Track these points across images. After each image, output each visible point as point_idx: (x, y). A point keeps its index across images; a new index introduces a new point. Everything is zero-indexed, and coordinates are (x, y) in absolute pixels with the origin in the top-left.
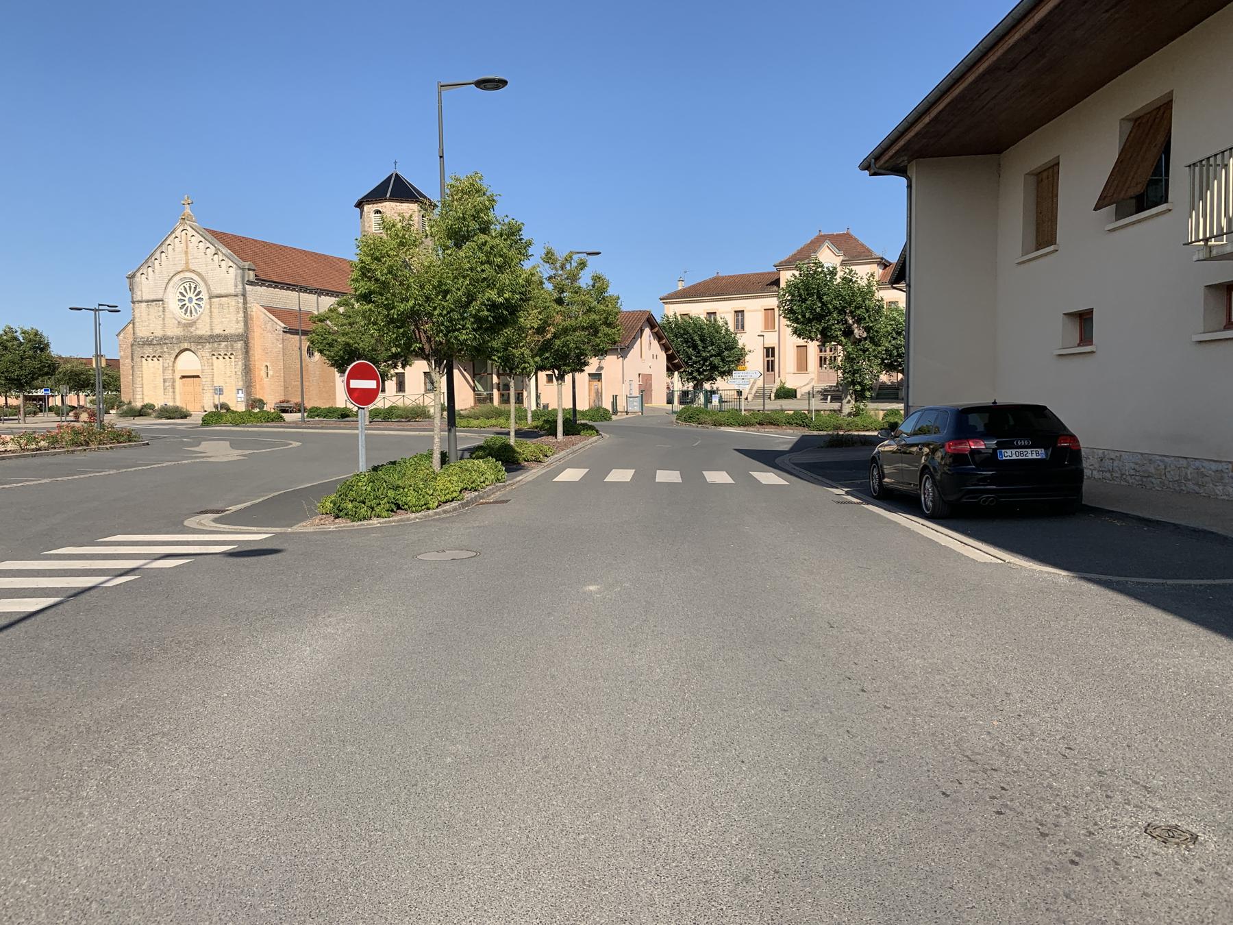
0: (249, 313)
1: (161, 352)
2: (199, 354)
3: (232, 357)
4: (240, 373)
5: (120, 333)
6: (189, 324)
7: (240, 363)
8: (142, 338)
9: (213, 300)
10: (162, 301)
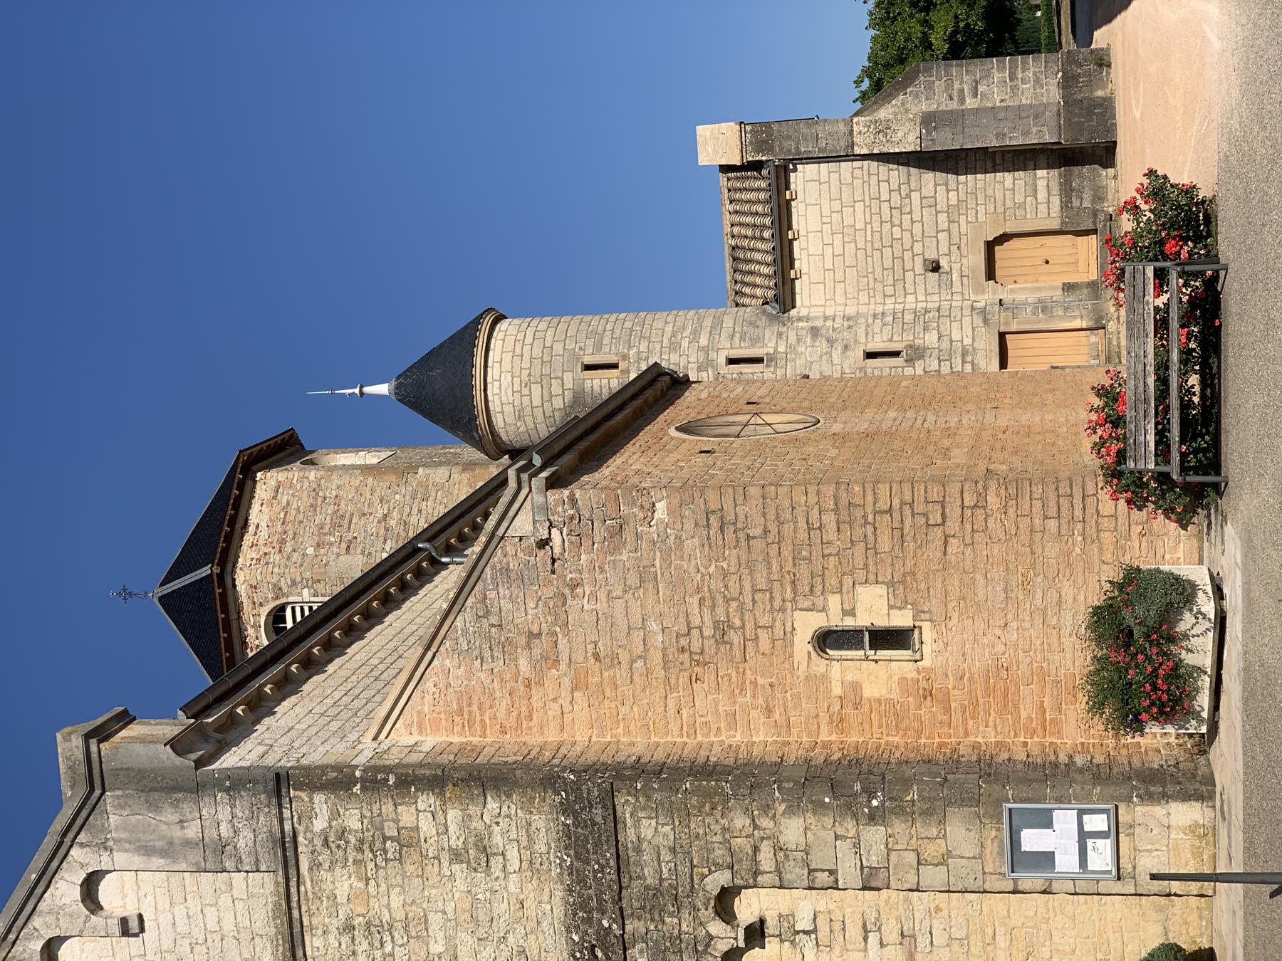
0: (414, 758)
3: (748, 908)
4: (874, 836)
7: (792, 830)
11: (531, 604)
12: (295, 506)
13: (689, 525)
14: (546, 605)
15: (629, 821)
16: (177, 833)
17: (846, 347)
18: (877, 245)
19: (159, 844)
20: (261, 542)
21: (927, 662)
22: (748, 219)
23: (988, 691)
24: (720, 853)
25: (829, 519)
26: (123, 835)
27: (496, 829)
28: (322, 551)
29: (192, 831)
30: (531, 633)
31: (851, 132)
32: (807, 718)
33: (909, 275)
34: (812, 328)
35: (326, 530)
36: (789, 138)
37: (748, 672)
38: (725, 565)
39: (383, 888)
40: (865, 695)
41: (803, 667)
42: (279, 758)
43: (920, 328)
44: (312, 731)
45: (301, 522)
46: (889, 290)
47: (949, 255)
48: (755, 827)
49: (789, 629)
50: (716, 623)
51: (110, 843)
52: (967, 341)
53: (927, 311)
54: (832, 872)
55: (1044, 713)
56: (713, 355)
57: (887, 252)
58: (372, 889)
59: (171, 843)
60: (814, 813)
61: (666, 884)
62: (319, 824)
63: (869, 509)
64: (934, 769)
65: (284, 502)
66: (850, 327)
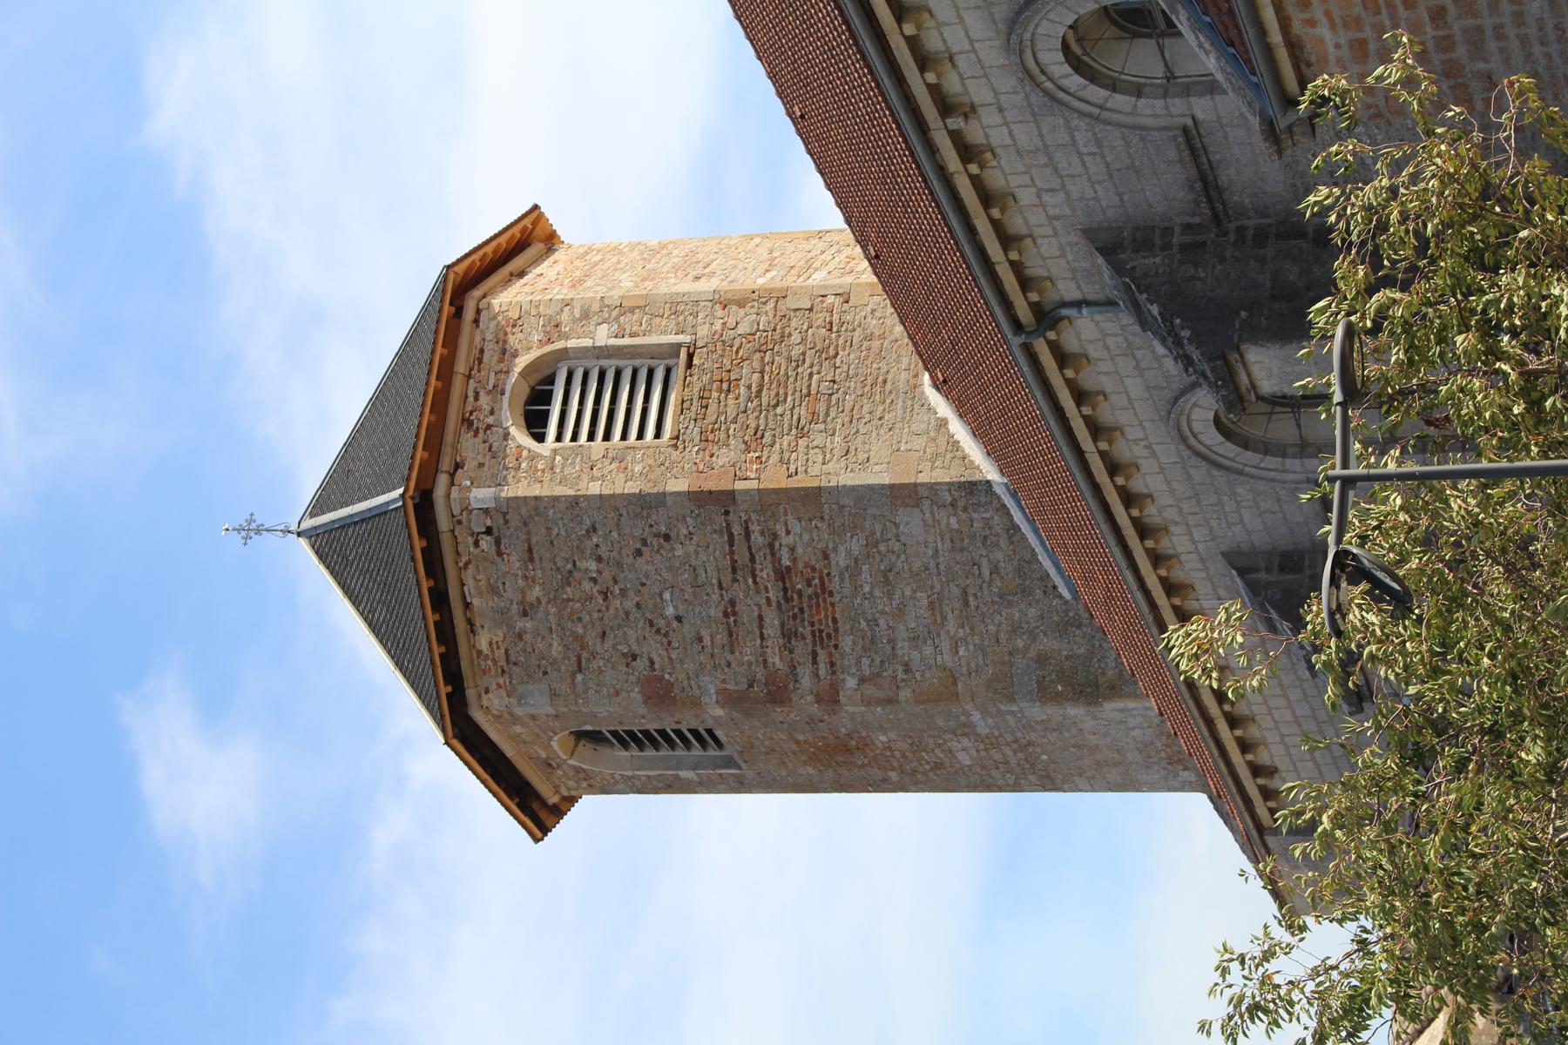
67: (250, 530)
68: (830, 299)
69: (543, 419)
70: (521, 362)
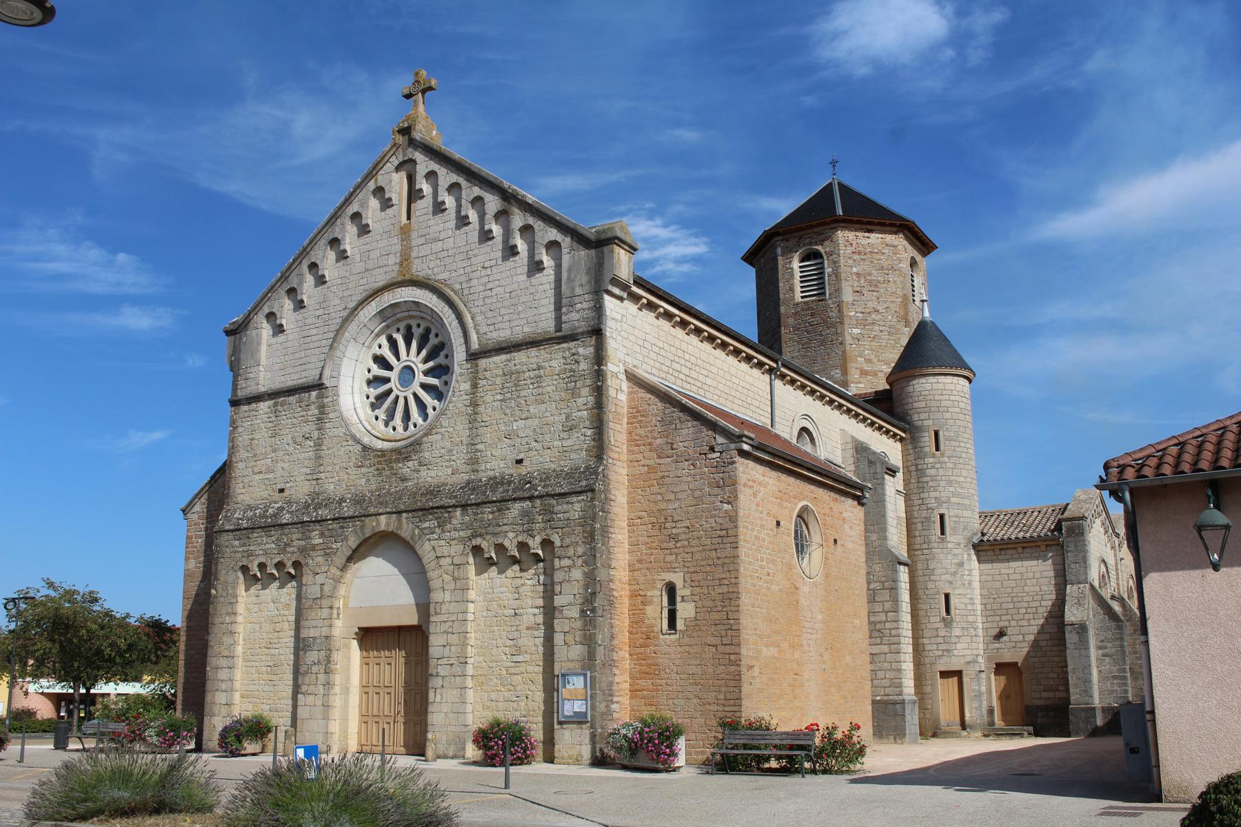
1: (303, 550)
2: (426, 549)
5: (191, 504)
6: (397, 451)
8: (250, 508)
9: (483, 363)
10: (319, 386)
11: (685, 444)
12: (882, 257)
13: (720, 521)
14: (686, 451)
15: (579, 498)
16: (577, 284)
17: (951, 583)
18: (1015, 599)
19: (573, 276)
20: (859, 241)
21: (661, 637)
22: (1037, 522)
23: (649, 666)
24: (567, 541)
25: (725, 589)
26: (576, 258)
27: (579, 435)
28: (854, 277)
29: (578, 291)
30: (672, 444)
31: (1080, 583)
32: (637, 579)
33: (998, 618)
34: (963, 563)
35: (867, 278)
36: (1076, 546)
37: (656, 551)
38: (704, 539)
39: (555, 382)
40: (647, 607)
41: (660, 577)
42: (610, 329)
43: (964, 625)
44: (633, 338)
45: (872, 262)
46: (989, 607)
47: (1010, 641)
48: (579, 557)
49: (676, 570)
50: (678, 534)
51: (573, 252)
52: (956, 652)
53: (975, 629)
54: (560, 592)
55: (639, 691)
56: (945, 505)
57: (1011, 605)
58: (555, 377)
59: (573, 281)
60: (585, 585)
61: (555, 516)
62: (581, 350)
63: (728, 608)
64: (607, 640)
65: (883, 251)
66: (964, 584)
67: (834, 163)
68: (840, 339)
69: (809, 259)
70: (820, 248)
